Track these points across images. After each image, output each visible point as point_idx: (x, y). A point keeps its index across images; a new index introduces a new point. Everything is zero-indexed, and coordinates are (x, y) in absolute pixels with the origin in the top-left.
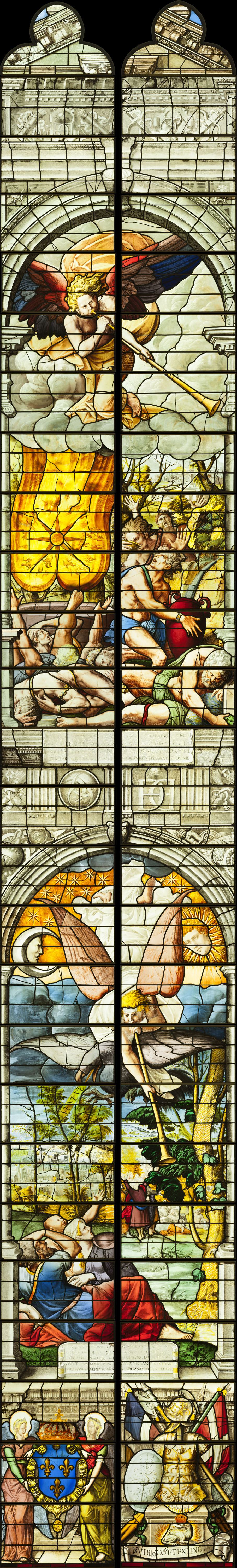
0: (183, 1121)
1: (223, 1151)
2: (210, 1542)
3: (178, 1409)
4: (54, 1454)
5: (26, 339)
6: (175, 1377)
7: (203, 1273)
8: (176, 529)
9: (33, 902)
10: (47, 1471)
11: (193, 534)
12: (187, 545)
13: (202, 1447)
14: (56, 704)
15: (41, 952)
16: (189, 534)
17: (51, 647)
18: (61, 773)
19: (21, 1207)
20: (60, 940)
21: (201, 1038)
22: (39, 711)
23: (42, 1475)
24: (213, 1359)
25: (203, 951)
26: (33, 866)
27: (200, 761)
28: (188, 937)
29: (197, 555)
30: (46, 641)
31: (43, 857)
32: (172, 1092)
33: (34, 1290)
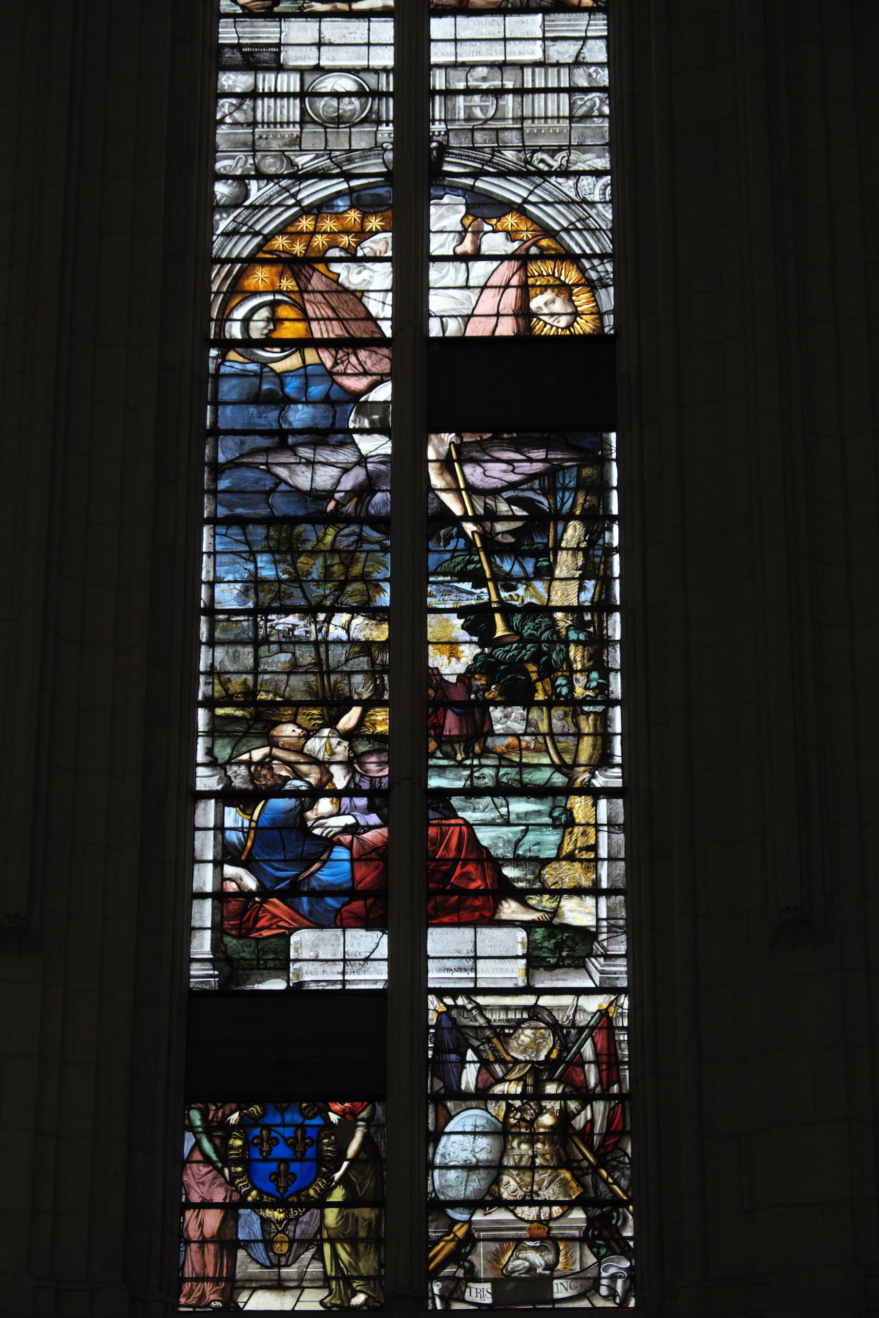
0: (532, 576)
1: (601, 622)
2: (591, 1273)
3: (527, 1040)
4: (278, 1120)
6: (521, 983)
7: (569, 812)
9: (261, 255)
10: (266, 1147)
13: (573, 1105)
15: (272, 327)
18: (308, 79)
19: (229, 711)
20: (304, 311)
21: (562, 450)
23: (257, 1155)
24: (590, 955)
25: (563, 321)
26: (262, 206)
27: (554, 57)
28: (536, 303)
31: (279, 193)
32: (511, 532)
33: (249, 844)
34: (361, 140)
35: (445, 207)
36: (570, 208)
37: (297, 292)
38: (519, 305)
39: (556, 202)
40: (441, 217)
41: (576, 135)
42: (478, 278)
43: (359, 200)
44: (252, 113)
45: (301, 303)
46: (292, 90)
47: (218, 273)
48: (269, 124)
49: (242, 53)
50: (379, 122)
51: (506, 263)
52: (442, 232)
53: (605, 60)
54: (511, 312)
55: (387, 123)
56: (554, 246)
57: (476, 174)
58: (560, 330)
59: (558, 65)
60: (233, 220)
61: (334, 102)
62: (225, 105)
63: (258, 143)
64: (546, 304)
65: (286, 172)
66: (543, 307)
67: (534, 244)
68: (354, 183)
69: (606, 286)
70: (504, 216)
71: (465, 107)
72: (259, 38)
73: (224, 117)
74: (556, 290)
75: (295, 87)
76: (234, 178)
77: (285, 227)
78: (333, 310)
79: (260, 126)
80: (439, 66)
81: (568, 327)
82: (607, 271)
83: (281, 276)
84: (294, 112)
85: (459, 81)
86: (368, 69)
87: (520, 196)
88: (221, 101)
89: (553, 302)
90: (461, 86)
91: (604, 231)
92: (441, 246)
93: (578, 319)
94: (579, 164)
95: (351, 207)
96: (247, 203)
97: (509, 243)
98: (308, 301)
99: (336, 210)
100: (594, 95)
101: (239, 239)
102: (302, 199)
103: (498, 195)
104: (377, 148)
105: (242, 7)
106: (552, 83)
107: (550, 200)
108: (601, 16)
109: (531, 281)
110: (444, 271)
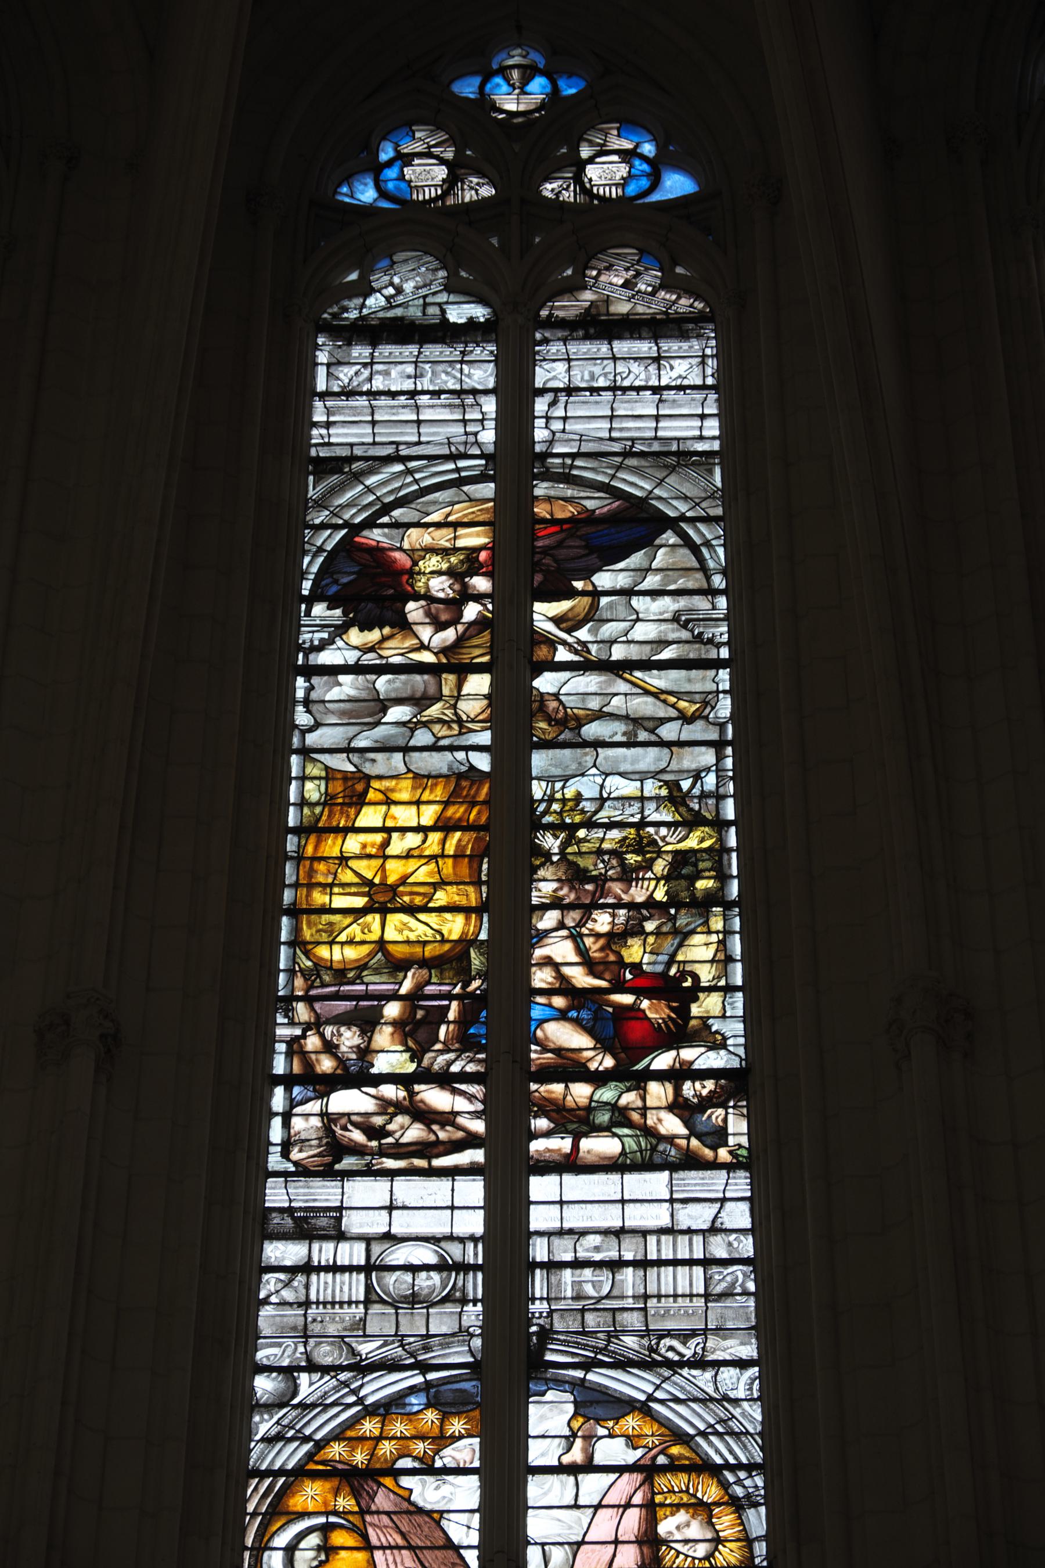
5: (340, 632)
8: (628, 876)
9: (312, 1466)
11: (663, 882)
12: (651, 896)
14: (370, 1139)
15: (323, 1557)
16: (653, 883)
17: (365, 1053)
18: (376, 1249)
20: (365, 1537)
22: (335, 1148)
25: (701, 1550)
26: (314, 1405)
27: (684, 1223)
28: (666, 1527)
29: (673, 911)
30: (357, 1041)
31: (336, 1389)
34: (442, 1322)
35: (547, 1406)
36: (708, 1407)
37: (356, 1513)
38: (643, 1529)
39: (689, 1400)
40: (543, 1418)
41: (714, 1317)
42: (590, 1494)
43: (437, 1397)
44: (304, 1291)
45: (362, 1528)
46: (355, 1263)
47: (256, 1489)
48: (325, 1304)
49: (293, 1218)
50: (464, 1301)
51: (626, 1476)
52: (543, 1437)
53: (749, 1226)
54: (633, 1539)
55: (475, 1302)
56: (687, 1455)
57: (587, 1365)
58: (697, 1561)
59: (689, 1231)
60: (277, 1423)
61: (408, 1277)
62: (270, 1283)
63: (310, 1327)
64: (678, 1528)
65: (346, 1363)
66: (675, 1532)
67: (662, 1452)
68: (432, 1376)
69: (756, 1505)
70: (623, 1417)
71: (573, 1282)
72: (315, 1200)
73: (269, 1296)
74: (691, 1511)
75: (359, 1260)
76: (280, 1370)
77: (343, 1432)
78: (403, 1535)
79: (314, 1306)
80: (540, 1234)
81: (707, 1558)
82: (756, 1487)
83: (336, 1493)
84: (357, 1290)
85: (565, 1252)
86: (451, 1238)
87: (644, 1392)
88: (266, 1277)
89: (688, 1525)
90: (568, 1257)
91: (751, 1435)
92: (543, 1455)
93: (720, 1547)
94: (718, 1352)
95: (428, 1406)
96: (295, 1401)
97: (630, 1451)
98: (371, 1524)
99: (408, 1409)
100: (735, 1268)
101: (284, 1445)
102: (366, 1396)
103: (615, 1390)
104: (463, 1333)
105: (296, 1163)
106: (683, 1254)
107: (682, 1396)
108: (742, 1173)
109: (658, 1499)
110: (546, 1487)
